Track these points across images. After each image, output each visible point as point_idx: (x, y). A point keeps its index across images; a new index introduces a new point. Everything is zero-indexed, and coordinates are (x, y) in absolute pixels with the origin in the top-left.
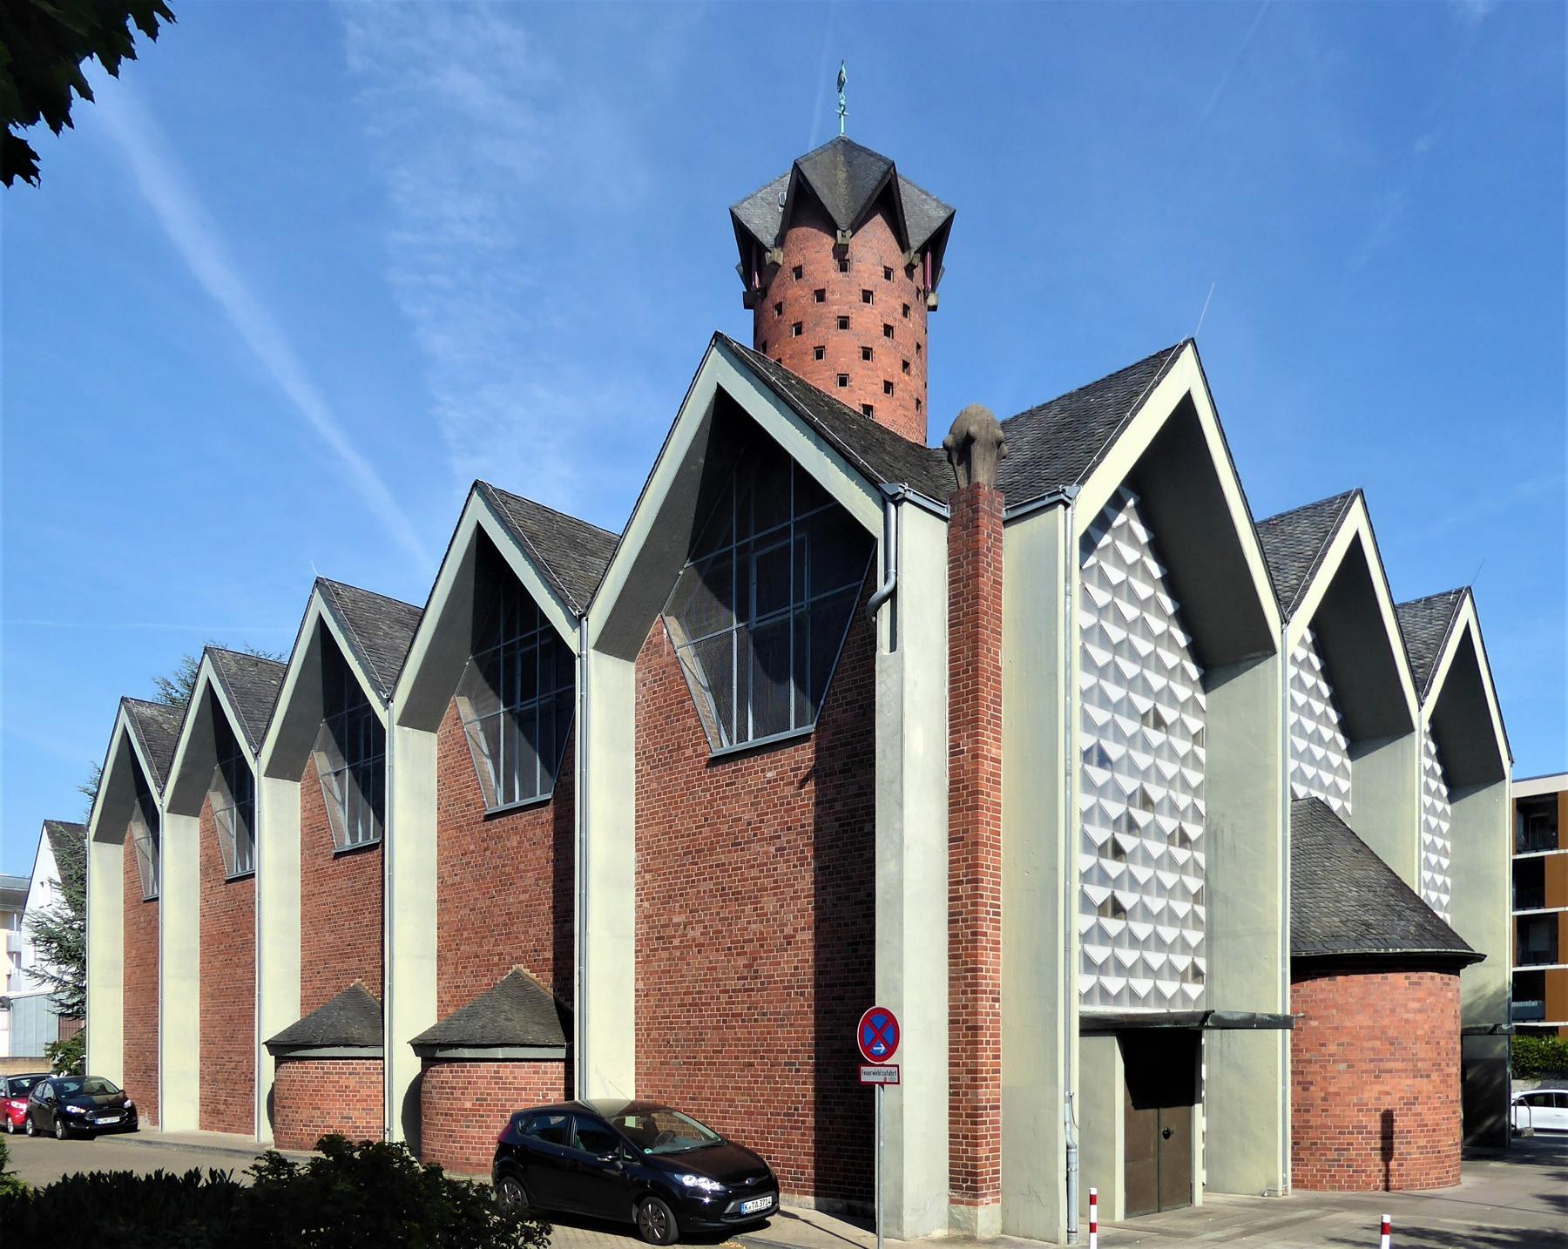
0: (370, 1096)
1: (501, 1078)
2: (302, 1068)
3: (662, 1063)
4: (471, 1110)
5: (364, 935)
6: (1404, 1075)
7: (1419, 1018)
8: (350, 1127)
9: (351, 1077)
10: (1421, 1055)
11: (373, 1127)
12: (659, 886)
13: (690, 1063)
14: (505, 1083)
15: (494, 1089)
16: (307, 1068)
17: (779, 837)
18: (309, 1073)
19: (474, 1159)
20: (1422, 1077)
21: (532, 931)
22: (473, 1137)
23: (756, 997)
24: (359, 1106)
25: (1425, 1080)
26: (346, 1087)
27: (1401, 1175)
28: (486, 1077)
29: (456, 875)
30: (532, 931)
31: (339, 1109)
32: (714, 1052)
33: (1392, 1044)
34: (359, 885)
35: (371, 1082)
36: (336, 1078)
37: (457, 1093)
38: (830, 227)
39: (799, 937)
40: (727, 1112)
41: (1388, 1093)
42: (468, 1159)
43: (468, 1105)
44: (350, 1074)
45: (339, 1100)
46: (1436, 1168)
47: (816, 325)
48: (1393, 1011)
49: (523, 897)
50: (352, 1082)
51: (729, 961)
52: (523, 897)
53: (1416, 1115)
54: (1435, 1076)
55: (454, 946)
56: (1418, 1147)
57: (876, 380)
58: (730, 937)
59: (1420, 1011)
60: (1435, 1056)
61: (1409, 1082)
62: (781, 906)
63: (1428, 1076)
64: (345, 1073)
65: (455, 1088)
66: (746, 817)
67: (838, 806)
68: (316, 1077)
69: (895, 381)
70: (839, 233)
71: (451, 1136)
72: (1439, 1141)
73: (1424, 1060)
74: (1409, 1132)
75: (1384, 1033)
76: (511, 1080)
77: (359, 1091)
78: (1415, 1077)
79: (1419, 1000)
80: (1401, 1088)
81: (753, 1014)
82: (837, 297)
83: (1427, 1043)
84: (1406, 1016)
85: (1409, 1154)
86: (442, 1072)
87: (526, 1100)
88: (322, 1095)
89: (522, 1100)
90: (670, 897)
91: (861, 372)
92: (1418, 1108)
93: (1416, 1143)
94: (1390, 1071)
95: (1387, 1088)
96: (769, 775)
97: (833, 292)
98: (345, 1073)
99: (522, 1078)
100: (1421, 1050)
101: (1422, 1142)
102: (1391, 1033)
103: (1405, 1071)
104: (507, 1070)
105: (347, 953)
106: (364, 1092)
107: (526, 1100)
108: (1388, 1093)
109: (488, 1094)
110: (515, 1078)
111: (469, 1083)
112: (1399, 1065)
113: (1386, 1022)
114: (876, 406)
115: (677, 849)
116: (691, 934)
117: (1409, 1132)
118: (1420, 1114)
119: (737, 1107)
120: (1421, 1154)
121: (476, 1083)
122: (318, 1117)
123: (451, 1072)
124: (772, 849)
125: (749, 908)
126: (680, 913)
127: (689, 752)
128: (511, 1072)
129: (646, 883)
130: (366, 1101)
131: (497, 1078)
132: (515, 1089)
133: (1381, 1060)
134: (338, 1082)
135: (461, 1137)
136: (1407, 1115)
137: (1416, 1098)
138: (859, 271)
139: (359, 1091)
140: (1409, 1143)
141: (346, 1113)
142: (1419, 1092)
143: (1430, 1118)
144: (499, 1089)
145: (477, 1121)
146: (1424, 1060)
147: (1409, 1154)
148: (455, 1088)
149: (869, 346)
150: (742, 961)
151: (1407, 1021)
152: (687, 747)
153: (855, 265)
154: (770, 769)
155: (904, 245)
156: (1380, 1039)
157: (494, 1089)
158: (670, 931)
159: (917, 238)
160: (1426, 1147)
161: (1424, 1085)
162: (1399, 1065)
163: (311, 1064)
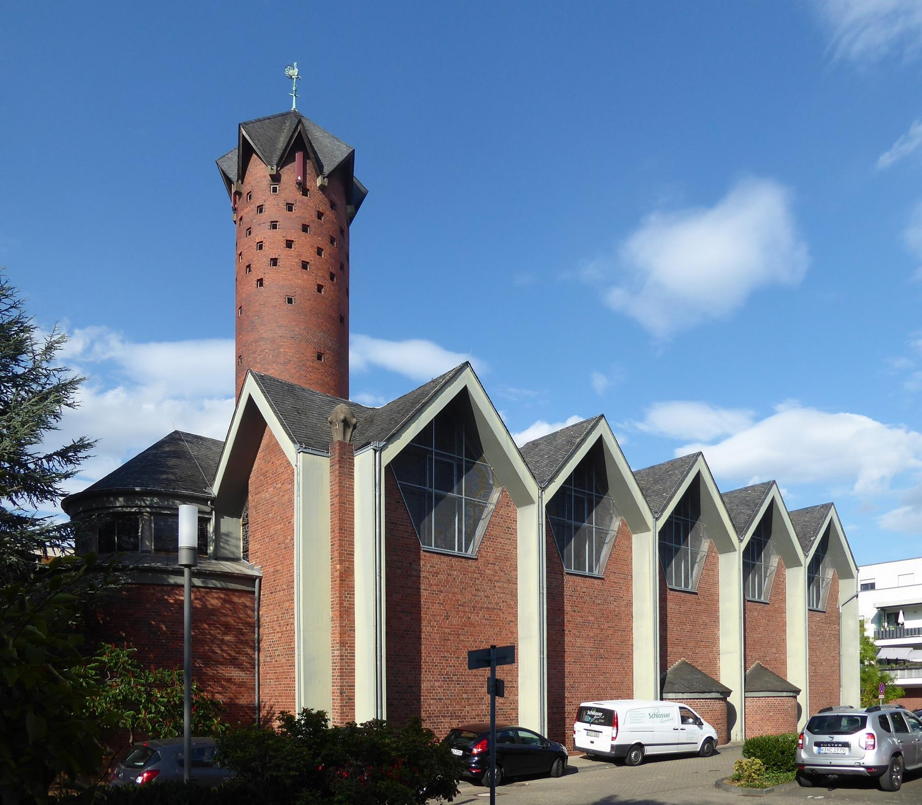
5: (687, 636)
21: (762, 649)
30: (762, 649)
34: (682, 610)
49: (759, 636)
52: (759, 636)
105: (675, 644)
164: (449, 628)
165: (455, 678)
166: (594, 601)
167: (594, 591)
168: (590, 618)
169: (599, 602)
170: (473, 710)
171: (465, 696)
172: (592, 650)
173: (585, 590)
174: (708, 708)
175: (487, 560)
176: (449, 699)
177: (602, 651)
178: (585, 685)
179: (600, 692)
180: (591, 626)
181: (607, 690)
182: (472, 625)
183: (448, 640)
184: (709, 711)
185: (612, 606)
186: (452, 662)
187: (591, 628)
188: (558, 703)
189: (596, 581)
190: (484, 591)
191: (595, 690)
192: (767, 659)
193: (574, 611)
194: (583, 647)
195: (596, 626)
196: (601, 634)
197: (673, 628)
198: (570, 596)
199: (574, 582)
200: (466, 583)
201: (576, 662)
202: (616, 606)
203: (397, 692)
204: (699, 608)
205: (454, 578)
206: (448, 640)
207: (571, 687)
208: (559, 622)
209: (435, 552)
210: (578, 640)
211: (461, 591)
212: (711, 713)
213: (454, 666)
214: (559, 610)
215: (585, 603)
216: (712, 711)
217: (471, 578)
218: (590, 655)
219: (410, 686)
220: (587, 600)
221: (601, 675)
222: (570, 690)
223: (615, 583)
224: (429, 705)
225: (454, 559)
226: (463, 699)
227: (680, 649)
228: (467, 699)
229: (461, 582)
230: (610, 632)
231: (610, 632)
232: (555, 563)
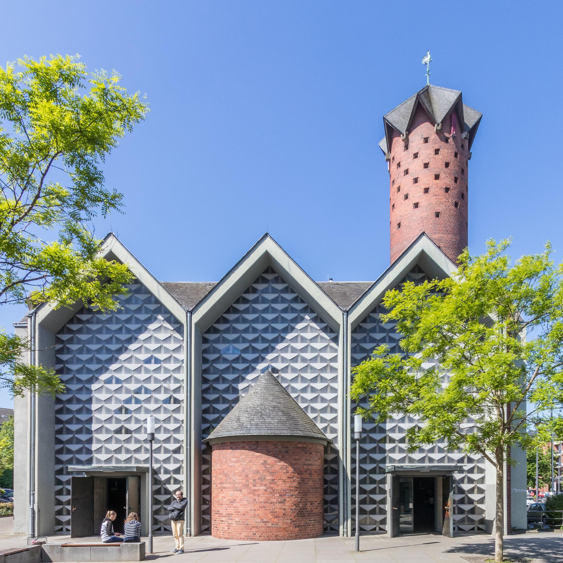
6: (229, 490)
7: (236, 464)
10: (237, 481)
20: (237, 491)
25: (239, 492)
27: (229, 533)
33: (226, 476)
41: (224, 497)
46: (245, 531)
47: (398, 178)
48: (226, 462)
53: (234, 507)
54: (245, 491)
56: (236, 522)
59: (237, 462)
60: (244, 481)
61: (232, 493)
63: (241, 490)
72: (247, 520)
73: (239, 483)
74: (232, 514)
75: (223, 472)
78: (234, 491)
79: (236, 457)
80: (228, 495)
82: (404, 162)
83: (240, 476)
84: (230, 464)
85: (232, 524)
92: (235, 504)
93: (235, 519)
94: (225, 488)
95: (224, 495)
100: (237, 479)
101: (237, 519)
102: (226, 471)
103: (230, 488)
108: (224, 497)
112: (228, 485)
113: (224, 467)
117: (232, 514)
118: (237, 507)
120: (237, 524)
133: (223, 483)
136: (230, 507)
137: (235, 500)
140: (232, 519)
142: (237, 497)
143: (241, 509)
146: (239, 483)
147: (232, 524)
149: (417, 177)
151: (231, 466)
153: (411, 145)
156: (222, 474)
160: (240, 522)
161: (237, 494)
162: (228, 485)
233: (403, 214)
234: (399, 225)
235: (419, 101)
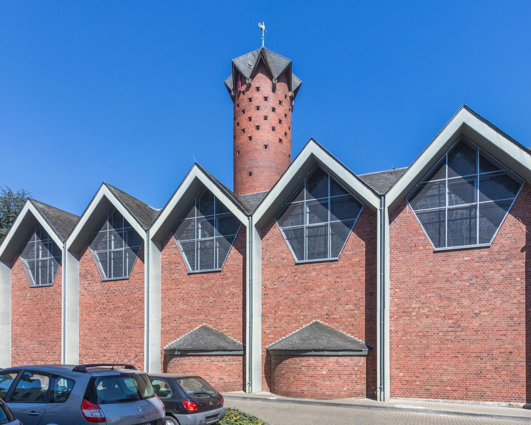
0: (230, 370)
1: (339, 362)
2: (199, 359)
3: (405, 356)
4: (325, 374)
8: (222, 383)
9: (223, 362)
11: (231, 382)
12: (403, 294)
13: (422, 356)
14: (340, 364)
15: (336, 366)
16: (202, 359)
17: (471, 280)
18: (203, 361)
19: (327, 393)
22: (327, 385)
23: (458, 334)
24: (226, 374)
26: (221, 366)
28: (333, 362)
29: (275, 285)
31: (218, 375)
32: (435, 352)
35: (231, 364)
36: (216, 363)
37: (319, 368)
38: (271, 77)
39: (482, 314)
40: (443, 373)
42: (324, 393)
43: (324, 373)
44: (223, 361)
45: (218, 372)
50: (223, 364)
51: (444, 321)
55: (273, 312)
57: (283, 131)
58: (444, 312)
62: (473, 303)
64: (220, 361)
65: (317, 366)
66: (453, 272)
67: (503, 271)
68: (207, 363)
69: (287, 133)
70: (274, 80)
71: (315, 385)
76: (343, 363)
77: (226, 368)
81: (458, 340)
86: (310, 360)
87: (348, 370)
88: (210, 370)
89: (347, 370)
90: (410, 298)
91: (279, 128)
96: (466, 259)
97: (270, 99)
98: (220, 361)
99: (347, 362)
104: (341, 359)
106: (228, 368)
107: (348, 370)
109: (334, 368)
110: (344, 362)
111: (325, 364)
114: (283, 140)
115: (414, 281)
116: (422, 311)
119: (449, 371)
121: (328, 364)
122: (208, 379)
123: (315, 360)
124: (468, 284)
125: (455, 304)
126: (416, 304)
127: (421, 248)
128: (343, 360)
129: (396, 292)
130: (229, 372)
131: (337, 362)
132: (344, 366)
134: (217, 365)
135: (320, 385)
138: (278, 94)
139: (226, 368)
141: (221, 377)
144: (338, 366)
145: (329, 379)
148: (317, 366)
150: (451, 321)
152: (420, 246)
154: (467, 257)
155: (290, 90)
157: (336, 366)
158: (411, 310)
159: (294, 88)
163: (205, 358)
164: (41, 320)
165: (43, 343)
166: (122, 294)
167: (123, 288)
168: (120, 305)
169: (126, 293)
170: (51, 358)
171: (47, 351)
172: (121, 324)
173: (115, 288)
174: (178, 362)
175: (58, 285)
176: (40, 352)
177: (128, 324)
178: (115, 345)
179: (126, 349)
180: (120, 309)
181: (132, 348)
182: (51, 317)
183: (40, 325)
184: (179, 364)
185: (137, 295)
186: (42, 335)
187: (120, 310)
188: (97, 355)
189: (124, 282)
190: (57, 300)
191: (122, 348)
192: (335, 316)
193: (108, 302)
194: (114, 323)
195: (124, 309)
196: (127, 313)
197: (194, 302)
198: (106, 294)
199: (108, 285)
200: (49, 298)
201: (109, 332)
202: (140, 294)
203: (21, 350)
204: (226, 281)
205: (43, 297)
206: (40, 325)
207: (105, 346)
208: (98, 310)
209: (246, 272)
210: (111, 319)
211: (46, 302)
212: (180, 366)
213: (43, 337)
214: (98, 303)
215: (116, 296)
216: (181, 364)
217: (51, 295)
218: (119, 327)
219: (25, 347)
220: (117, 294)
221: (127, 339)
222: (105, 348)
223: (139, 279)
224: (32, 355)
225: (44, 288)
226: (46, 352)
227: (202, 317)
228: (48, 352)
229: (46, 298)
230: (134, 311)
231: (134, 311)
232: (96, 277)
233: (271, 141)
234: (266, 147)
235: (290, 67)
